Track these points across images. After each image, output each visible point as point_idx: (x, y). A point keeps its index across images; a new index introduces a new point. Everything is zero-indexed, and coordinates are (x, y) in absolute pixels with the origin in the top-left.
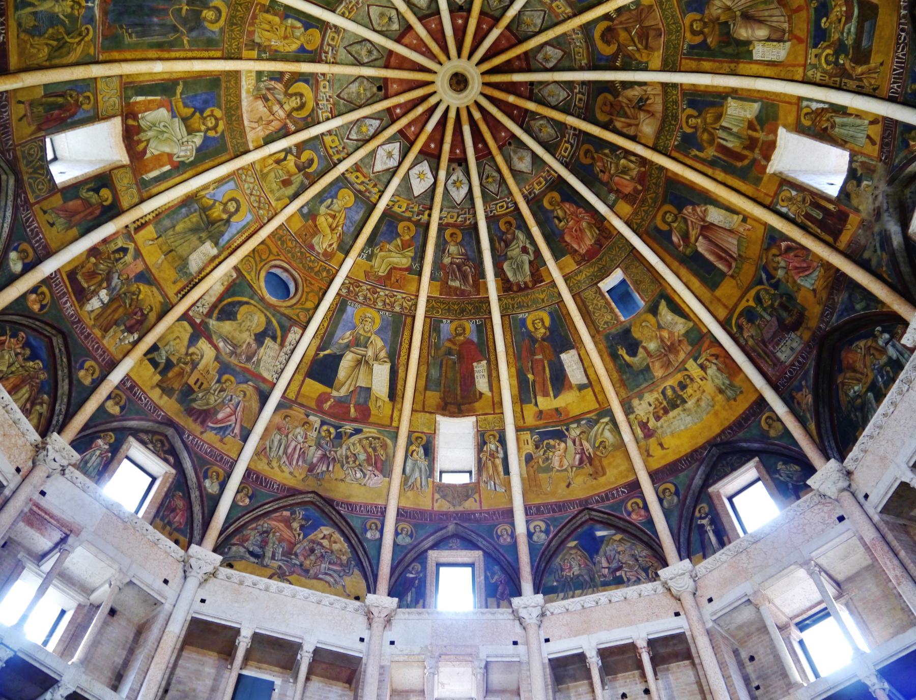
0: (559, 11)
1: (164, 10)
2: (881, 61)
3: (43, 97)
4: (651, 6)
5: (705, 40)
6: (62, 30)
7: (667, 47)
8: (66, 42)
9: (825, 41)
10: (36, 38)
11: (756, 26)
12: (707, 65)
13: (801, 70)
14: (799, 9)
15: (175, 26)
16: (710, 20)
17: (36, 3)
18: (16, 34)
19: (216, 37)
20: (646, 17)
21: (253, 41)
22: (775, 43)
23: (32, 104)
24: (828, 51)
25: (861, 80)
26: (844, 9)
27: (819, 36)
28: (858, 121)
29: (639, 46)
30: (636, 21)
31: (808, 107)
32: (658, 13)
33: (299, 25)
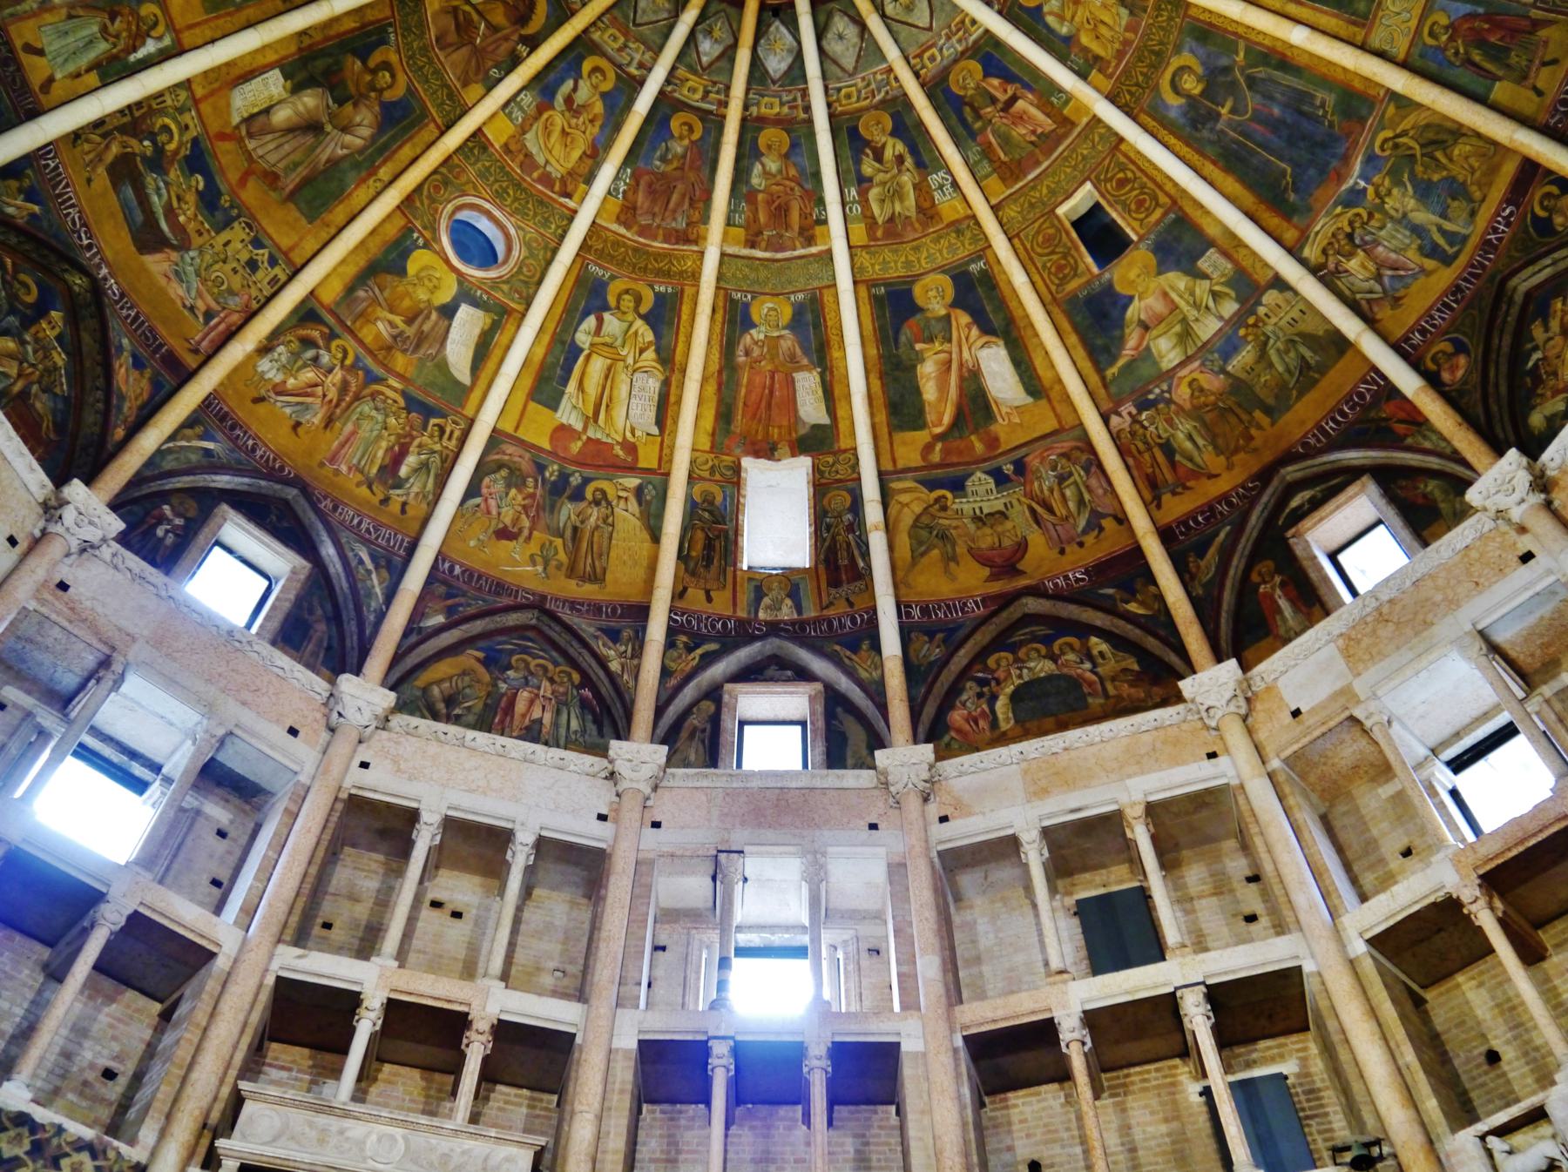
0: (611, 31)
1: (1260, 122)
2: (93, 185)
3: (1500, 79)
4: (465, 84)
5: (364, 62)
6: (1419, 169)
7: (422, 25)
8: (1422, 146)
9: (186, 157)
10: (1461, 178)
11: (295, 119)
12: (351, 24)
13: (199, 92)
14: (243, 181)
15: (1250, 87)
16: (367, 97)
17: (1434, 229)
18: (1484, 206)
19: (1189, 42)
20: (469, 62)
21: (1131, 13)
22: (256, 110)
23: (1522, 78)
24: (172, 146)
25: (104, 136)
26: (182, 219)
27: (197, 160)
28: (71, 68)
29: (467, 8)
30: (484, 49)
31: (160, 38)
32: (452, 77)
33: (1050, 20)
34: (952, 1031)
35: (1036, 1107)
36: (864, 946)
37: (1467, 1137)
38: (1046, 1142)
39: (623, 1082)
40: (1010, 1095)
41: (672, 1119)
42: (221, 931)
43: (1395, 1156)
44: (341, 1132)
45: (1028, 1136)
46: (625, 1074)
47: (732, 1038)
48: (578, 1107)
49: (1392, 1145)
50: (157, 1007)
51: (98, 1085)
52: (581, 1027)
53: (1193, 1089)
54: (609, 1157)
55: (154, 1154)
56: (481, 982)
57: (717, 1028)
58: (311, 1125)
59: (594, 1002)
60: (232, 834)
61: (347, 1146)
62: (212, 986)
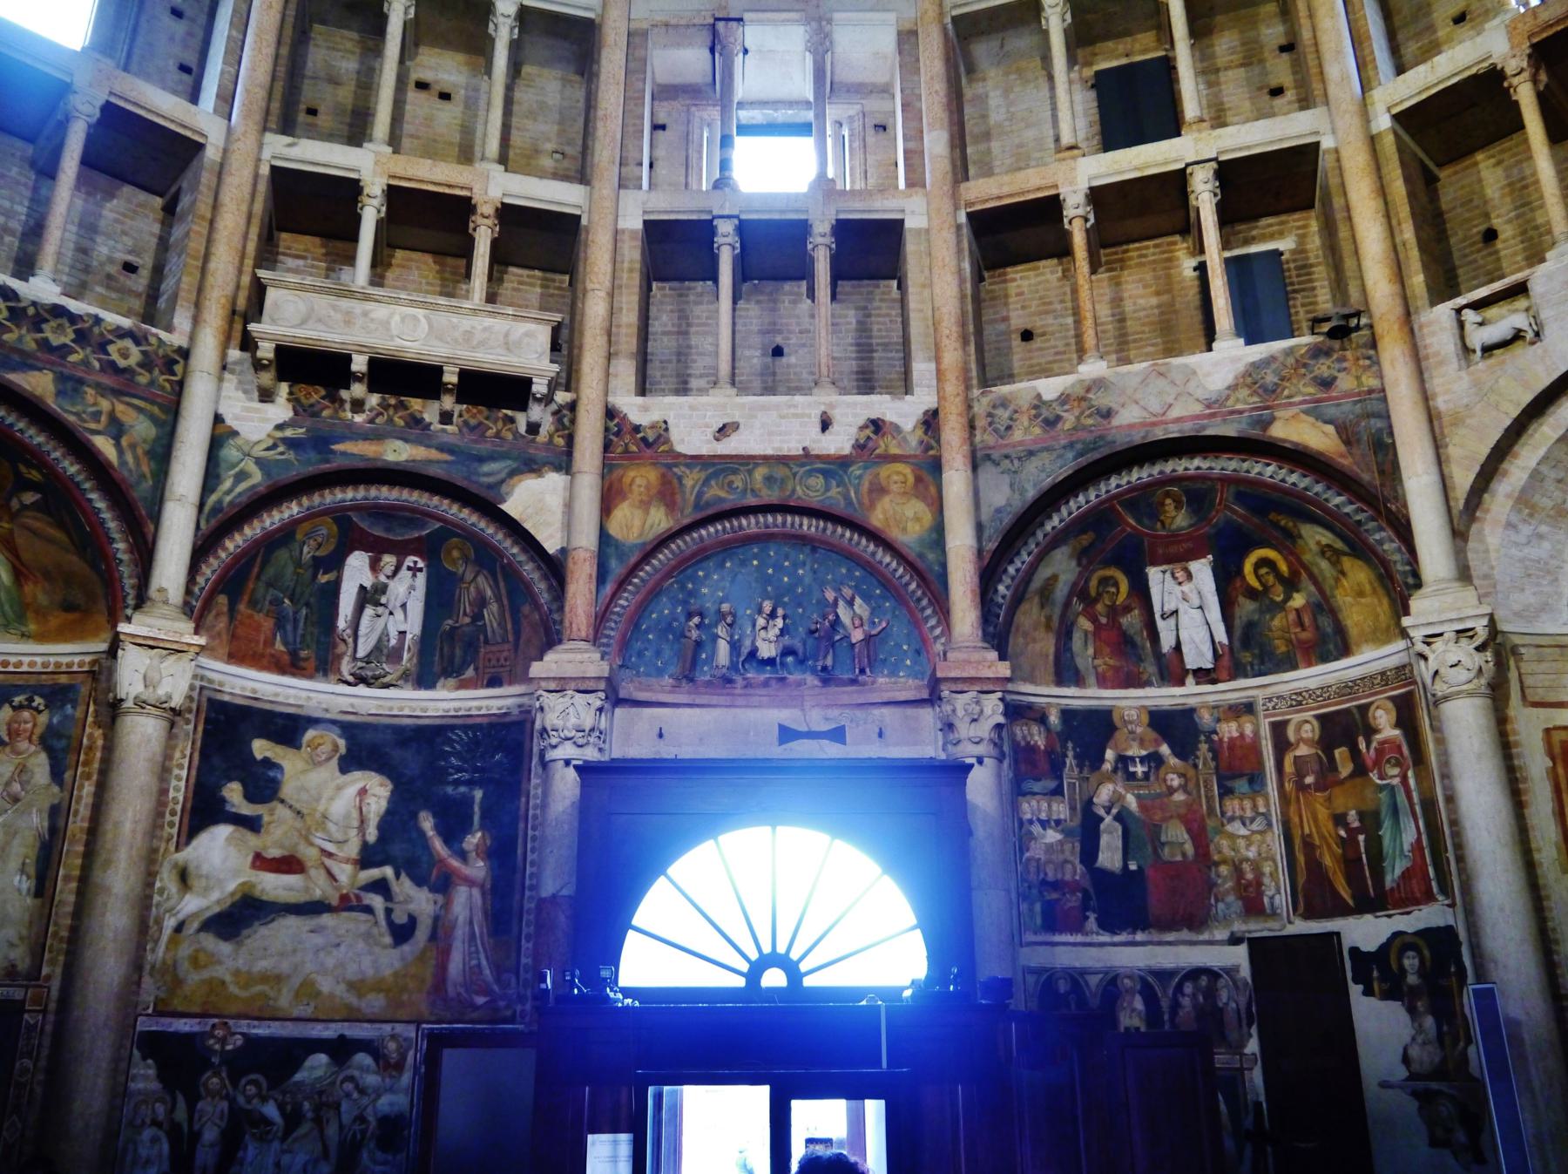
34: (956, 208)
35: (1033, 281)
36: (870, 122)
37: (1445, 310)
38: (1040, 313)
39: (631, 261)
40: (1009, 269)
41: (681, 295)
42: (201, 119)
43: (1371, 326)
44: (365, 314)
45: (1023, 308)
46: (632, 253)
47: (737, 217)
48: (589, 286)
49: (1371, 317)
50: (158, 202)
51: (122, 278)
52: (586, 208)
53: (1187, 266)
54: (624, 330)
55: (192, 338)
56: (480, 166)
57: (722, 207)
58: (334, 308)
59: (596, 183)
60: (188, 12)
61: (372, 326)
62: (207, 178)
